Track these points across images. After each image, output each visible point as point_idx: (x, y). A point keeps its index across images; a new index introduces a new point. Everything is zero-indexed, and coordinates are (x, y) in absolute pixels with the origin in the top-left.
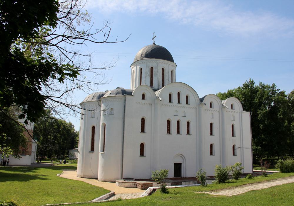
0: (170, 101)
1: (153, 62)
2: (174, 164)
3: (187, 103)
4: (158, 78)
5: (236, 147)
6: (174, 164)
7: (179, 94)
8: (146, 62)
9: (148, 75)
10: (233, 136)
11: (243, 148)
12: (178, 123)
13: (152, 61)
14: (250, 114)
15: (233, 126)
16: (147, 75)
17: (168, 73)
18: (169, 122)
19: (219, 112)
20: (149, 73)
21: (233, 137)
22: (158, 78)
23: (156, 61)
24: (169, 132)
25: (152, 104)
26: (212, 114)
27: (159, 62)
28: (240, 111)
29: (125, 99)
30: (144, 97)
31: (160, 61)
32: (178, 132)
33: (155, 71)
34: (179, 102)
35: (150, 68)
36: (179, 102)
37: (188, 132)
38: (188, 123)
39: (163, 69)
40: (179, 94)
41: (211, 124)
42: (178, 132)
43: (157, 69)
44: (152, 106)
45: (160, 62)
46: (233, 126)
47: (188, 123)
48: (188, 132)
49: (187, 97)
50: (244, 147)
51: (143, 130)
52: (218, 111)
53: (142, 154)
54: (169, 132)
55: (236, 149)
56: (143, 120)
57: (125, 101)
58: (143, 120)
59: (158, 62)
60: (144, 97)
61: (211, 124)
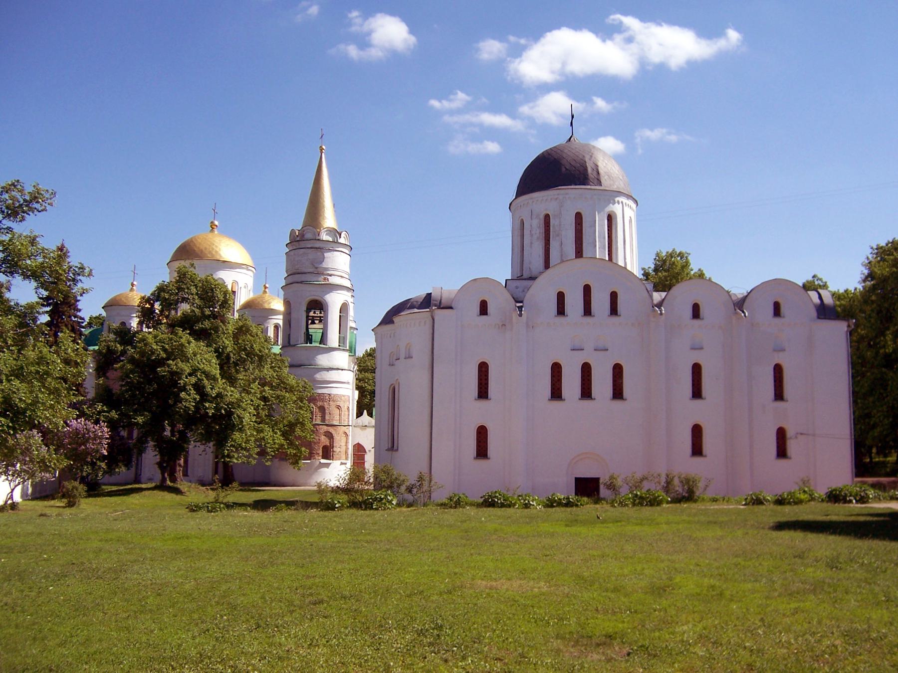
0: (561, 311)
3: (614, 311)
5: (790, 433)
7: (587, 290)
8: (530, 202)
9: (538, 238)
11: (814, 435)
12: (586, 370)
14: (849, 326)
16: (535, 237)
18: (556, 370)
20: (539, 232)
21: (779, 404)
23: (556, 197)
24: (556, 393)
25: (505, 325)
30: (484, 309)
32: (586, 392)
34: (588, 311)
35: (542, 217)
36: (588, 311)
37: (618, 393)
38: (618, 370)
39: (579, 217)
40: (587, 290)
41: (697, 370)
42: (586, 392)
45: (567, 196)
46: (778, 370)
47: (618, 370)
48: (618, 393)
49: (614, 296)
51: (483, 393)
53: (482, 452)
54: (556, 393)
56: (483, 369)
58: (483, 369)
59: (561, 197)
60: (484, 309)
61: (697, 370)
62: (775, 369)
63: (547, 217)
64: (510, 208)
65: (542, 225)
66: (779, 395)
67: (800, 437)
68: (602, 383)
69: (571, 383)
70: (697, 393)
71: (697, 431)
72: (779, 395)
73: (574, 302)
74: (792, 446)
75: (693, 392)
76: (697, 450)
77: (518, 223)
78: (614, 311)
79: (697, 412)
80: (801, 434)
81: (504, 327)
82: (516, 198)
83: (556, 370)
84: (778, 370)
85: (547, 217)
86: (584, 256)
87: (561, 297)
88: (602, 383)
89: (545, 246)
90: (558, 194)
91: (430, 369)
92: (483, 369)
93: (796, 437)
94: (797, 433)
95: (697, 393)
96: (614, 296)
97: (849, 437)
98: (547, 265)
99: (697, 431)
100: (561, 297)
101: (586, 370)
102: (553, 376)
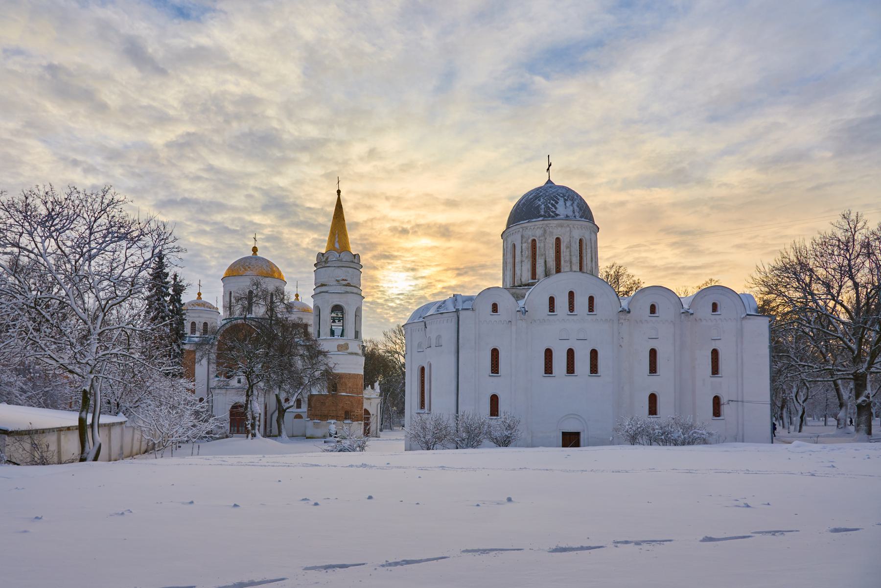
2: (564, 434)
4: (545, 261)
6: (564, 434)
7: (571, 294)
9: (527, 257)
12: (571, 353)
17: (570, 245)
18: (549, 353)
20: (528, 253)
21: (716, 379)
22: (545, 261)
29: (458, 318)
30: (495, 308)
32: (571, 369)
33: (539, 247)
35: (530, 241)
38: (594, 354)
40: (571, 294)
41: (653, 353)
42: (571, 369)
44: (511, 324)
46: (715, 353)
47: (594, 354)
55: (723, 404)
56: (495, 353)
57: (458, 320)
58: (495, 353)
60: (495, 308)
61: (653, 353)
62: (712, 353)
64: (502, 235)
65: (530, 249)
66: (715, 370)
68: (582, 362)
69: (560, 362)
70: (653, 369)
71: (653, 398)
72: (715, 370)
73: (562, 303)
74: (725, 409)
75: (650, 370)
76: (653, 411)
77: (510, 246)
78: (591, 308)
79: (653, 384)
81: (510, 323)
82: (508, 227)
83: (549, 353)
84: (715, 353)
85: (534, 241)
86: (562, 270)
87: (552, 300)
88: (582, 362)
89: (532, 263)
91: (456, 354)
92: (495, 354)
93: (728, 403)
95: (653, 369)
96: (591, 299)
98: (534, 276)
99: (653, 398)
100: (552, 300)
101: (571, 353)
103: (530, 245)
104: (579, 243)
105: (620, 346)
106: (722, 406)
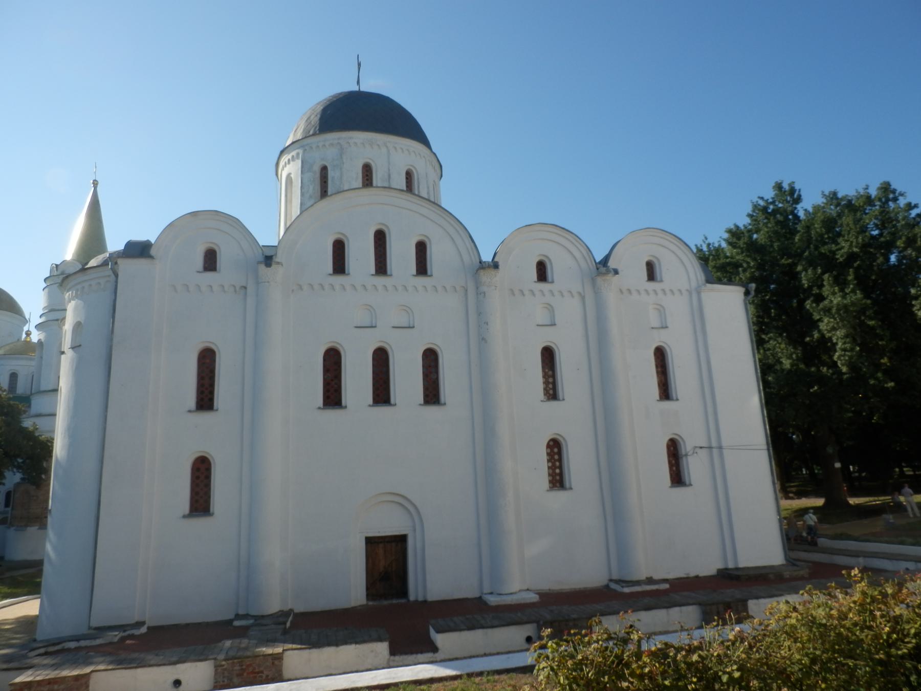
1: (324, 146)
7: (380, 238)
9: (311, 197)
10: (665, 392)
13: (321, 144)
14: (747, 293)
15: (660, 355)
19: (583, 298)
21: (666, 404)
26: (550, 308)
27: (348, 143)
28: (694, 284)
31: (351, 138)
33: (333, 178)
37: (432, 395)
38: (431, 359)
40: (380, 238)
41: (548, 356)
43: (341, 169)
46: (660, 355)
47: (431, 359)
48: (432, 395)
49: (421, 248)
50: (725, 443)
52: (579, 293)
55: (686, 455)
61: (548, 356)
63: (324, 169)
67: (698, 450)
71: (555, 448)
75: (546, 391)
78: (422, 268)
80: (701, 448)
85: (324, 169)
87: (339, 248)
90: (339, 139)
94: (696, 447)
96: (421, 248)
97: (765, 447)
99: (555, 448)
100: (339, 248)
102: (326, 370)
103: (318, 175)
104: (407, 178)
105: (483, 339)
106: (684, 459)
